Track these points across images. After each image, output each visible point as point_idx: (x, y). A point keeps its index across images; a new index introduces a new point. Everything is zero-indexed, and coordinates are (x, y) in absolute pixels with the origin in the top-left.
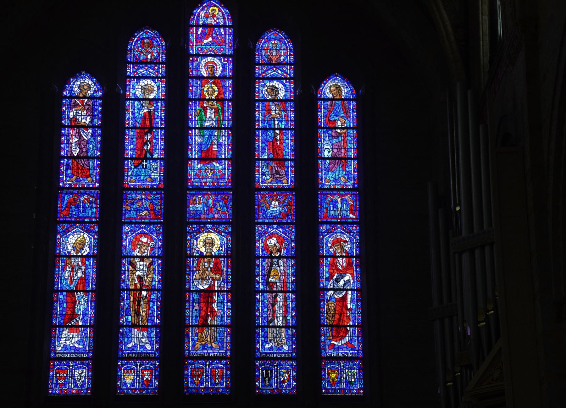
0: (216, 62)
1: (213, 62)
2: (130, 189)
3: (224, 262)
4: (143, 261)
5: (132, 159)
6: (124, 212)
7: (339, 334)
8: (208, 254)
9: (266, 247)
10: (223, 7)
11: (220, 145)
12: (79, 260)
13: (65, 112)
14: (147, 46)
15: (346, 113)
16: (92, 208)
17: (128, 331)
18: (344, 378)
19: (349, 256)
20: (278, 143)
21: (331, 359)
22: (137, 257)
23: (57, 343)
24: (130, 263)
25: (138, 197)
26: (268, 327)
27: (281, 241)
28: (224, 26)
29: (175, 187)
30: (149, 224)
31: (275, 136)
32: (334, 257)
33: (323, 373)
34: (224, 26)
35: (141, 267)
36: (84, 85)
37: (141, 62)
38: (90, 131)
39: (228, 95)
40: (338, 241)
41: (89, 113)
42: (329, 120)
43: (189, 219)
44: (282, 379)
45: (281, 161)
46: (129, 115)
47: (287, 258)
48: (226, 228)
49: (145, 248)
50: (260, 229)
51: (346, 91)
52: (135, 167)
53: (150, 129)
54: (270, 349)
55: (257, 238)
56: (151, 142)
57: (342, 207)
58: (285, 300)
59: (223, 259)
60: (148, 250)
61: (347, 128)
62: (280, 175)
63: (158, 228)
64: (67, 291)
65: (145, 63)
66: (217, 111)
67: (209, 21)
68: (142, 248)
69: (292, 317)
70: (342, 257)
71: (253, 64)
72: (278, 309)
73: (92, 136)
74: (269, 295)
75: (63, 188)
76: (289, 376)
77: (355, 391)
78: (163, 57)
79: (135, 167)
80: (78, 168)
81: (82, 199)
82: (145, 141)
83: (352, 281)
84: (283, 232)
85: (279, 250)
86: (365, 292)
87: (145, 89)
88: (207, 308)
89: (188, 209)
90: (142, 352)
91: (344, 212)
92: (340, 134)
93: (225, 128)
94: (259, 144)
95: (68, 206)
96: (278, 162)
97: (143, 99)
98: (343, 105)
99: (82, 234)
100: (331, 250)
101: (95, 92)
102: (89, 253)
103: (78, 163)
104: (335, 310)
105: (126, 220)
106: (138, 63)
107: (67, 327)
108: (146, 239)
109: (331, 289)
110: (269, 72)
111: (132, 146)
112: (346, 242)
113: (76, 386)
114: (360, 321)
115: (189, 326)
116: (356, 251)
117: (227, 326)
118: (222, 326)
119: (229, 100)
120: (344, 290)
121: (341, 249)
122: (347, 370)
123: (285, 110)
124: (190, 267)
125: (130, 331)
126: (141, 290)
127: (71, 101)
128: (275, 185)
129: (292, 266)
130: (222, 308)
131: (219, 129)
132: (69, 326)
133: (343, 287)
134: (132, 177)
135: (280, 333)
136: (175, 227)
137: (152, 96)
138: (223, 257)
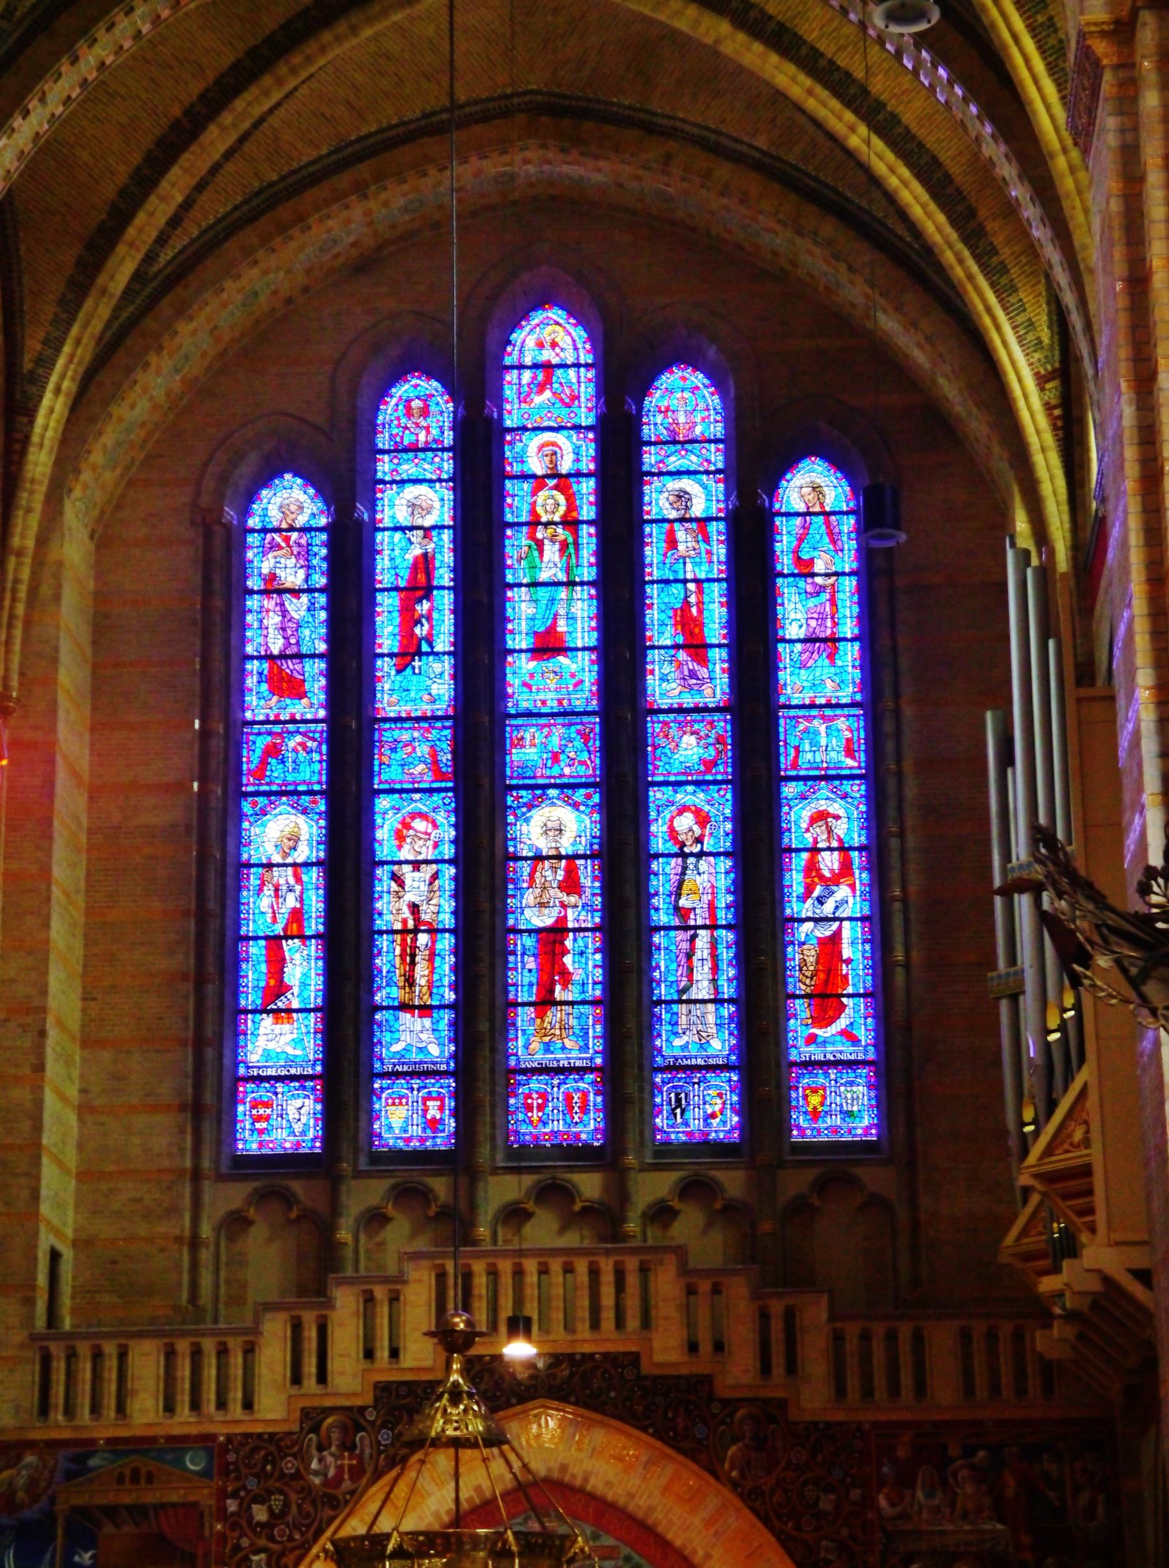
1: (554, 444)
5: (391, 655)
6: (376, 768)
7: (826, 1011)
8: (553, 852)
9: (673, 834)
11: (571, 618)
14: (417, 411)
15: (833, 542)
16: (311, 761)
17: (391, 1018)
19: (843, 849)
20: (694, 610)
21: (810, 1065)
22: (407, 862)
23: (250, 1047)
24: (395, 877)
26: (680, 1001)
27: (703, 820)
28: (577, 365)
30: (430, 791)
31: (686, 597)
32: (814, 850)
33: (794, 1095)
34: (577, 365)
35: (415, 882)
37: (406, 450)
38: (304, 598)
39: (587, 512)
40: (821, 816)
41: (302, 562)
42: (799, 558)
43: (512, 778)
45: (697, 647)
46: (382, 562)
47: (716, 855)
48: (588, 796)
49: (421, 842)
50: (659, 795)
51: (833, 494)
52: (399, 672)
54: (685, 1047)
55: (653, 815)
56: (429, 618)
59: (582, 862)
61: (837, 574)
63: (447, 801)
64: (266, 938)
65: (414, 448)
66: (564, 546)
67: (547, 355)
68: (415, 841)
69: (730, 980)
74: (681, 935)
75: (254, 723)
76: (724, 1103)
77: (860, 1131)
78: (448, 438)
79: (399, 672)
80: (281, 679)
81: (292, 744)
83: (851, 900)
84: (708, 802)
85: (699, 840)
86: (879, 926)
87: (415, 507)
88: (553, 965)
89: (508, 758)
90: (421, 1062)
91: (833, 754)
92: (822, 588)
93: (582, 584)
94: (653, 616)
95: (264, 762)
98: (827, 524)
99: (293, 818)
100: (808, 835)
101: (314, 515)
103: (280, 669)
104: (817, 963)
105: (382, 786)
106: (398, 449)
107: (268, 1012)
109: (808, 919)
110: (672, 459)
111: (390, 629)
113: (293, 1133)
114: (869, 985)
115: (516, 1004)
117: (594, 1003)
118: (583, 1002)
120: (835, 919)
123: (707, 540)
125: (397, 1019)
126: (416, 931)
128: (688, 701)
129: (727, 873)
130: (584, 964)
131: (570, 584)
137: (428, 522)
138: (584, 857)
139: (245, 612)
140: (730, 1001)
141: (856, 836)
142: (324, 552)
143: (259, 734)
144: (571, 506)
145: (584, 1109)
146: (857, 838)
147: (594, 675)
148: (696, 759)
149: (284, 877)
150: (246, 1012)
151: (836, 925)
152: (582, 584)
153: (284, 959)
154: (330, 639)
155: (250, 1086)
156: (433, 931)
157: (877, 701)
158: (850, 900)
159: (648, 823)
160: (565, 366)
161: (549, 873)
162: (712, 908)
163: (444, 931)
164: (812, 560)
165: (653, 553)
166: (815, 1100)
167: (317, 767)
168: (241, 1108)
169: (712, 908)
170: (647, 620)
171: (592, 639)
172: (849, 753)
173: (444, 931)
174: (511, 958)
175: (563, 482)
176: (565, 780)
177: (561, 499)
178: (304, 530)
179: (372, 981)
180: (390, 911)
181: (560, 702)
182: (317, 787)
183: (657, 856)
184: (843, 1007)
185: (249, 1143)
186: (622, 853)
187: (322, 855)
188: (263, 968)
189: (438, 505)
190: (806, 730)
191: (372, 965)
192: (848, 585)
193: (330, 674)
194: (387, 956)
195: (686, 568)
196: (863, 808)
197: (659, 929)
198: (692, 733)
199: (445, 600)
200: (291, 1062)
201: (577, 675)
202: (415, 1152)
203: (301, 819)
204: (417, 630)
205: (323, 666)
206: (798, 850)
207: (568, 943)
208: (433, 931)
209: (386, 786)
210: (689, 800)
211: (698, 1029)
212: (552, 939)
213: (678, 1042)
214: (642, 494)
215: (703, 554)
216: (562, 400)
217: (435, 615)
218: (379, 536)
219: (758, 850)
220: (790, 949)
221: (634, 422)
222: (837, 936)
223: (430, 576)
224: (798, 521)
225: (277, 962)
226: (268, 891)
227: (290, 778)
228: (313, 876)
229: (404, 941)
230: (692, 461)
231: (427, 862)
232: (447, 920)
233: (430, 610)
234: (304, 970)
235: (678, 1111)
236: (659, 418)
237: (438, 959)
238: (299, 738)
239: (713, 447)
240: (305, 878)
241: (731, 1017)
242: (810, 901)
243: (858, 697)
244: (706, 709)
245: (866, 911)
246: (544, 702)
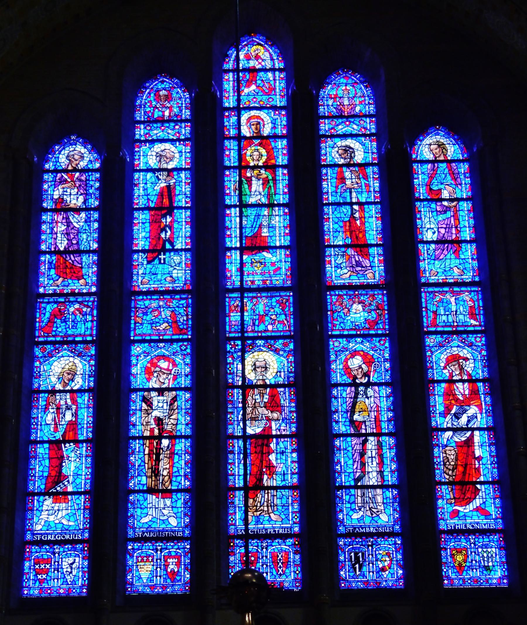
0: (262, 117)
1: (258, 117)
2: (141, 293)
3: (285, 393)
4: (163, 395)
6: (132, 326)
7: (464, 494)
8: (260, 383)
9: (347, 370)
10: (271, 46)
13: (47, 191)
15: (455, 179)
16: (86, 321)
17: (141, 498)
20: (358, 222)
21: (455, 532)
22: (154, 389)
23: (36, 519)
24: (145, 400)
25: (154, 304)
26: (356, 487)
27: (368, 360)
28: (273, 70)
29: (208, 289)
30: (171, 341)
31: (352, 214)
34: (273, 70)
36: (76, 154)
37: (156, 121)
38: (83, 215)
39: (282, 160)
41: (82, 191)
42: (431, 189)
43: (230, 332)
44: (381, 566)
45: (362, 247)
46: (138, 191)
47: (379, 384)
48: (285, 345)
49: (165, 376)
50: (336, 344)
51: (453, 149)
52: (149, 262)
53: (170, 210)
55: (333, 357)
56: (171, 227)
57: (457, 309)
58: (380, 446)
59: (282, 389)
60: (169, 380)
62: (362, 267)
63: (183, 348)
64: (49, 442)
65: (161, 121)
66: (266, 181)
67: (252, 63)
68: (160, 376)
69: (392, 472)
70: (463, 381)
72: (370, 460)
73: (86, 221)
74: (355, 441)
75: (44, 295)
76: (391, 560)
77: (495, 581)
78: (186, 114)
79: (149, 262)
81: (72, 310)
82: (162, 225)
84: (372, 349)
85: (367, 375)
86: (501, 433)
87: (162, 157)
88: (262, 462)
89: (227, 319)
90: (163, 530)
91: (461, 317)
92: (448, 209)
93: (279, 205)
94: (330, 226)
95: (51, 321)
96: (358, 249)
97: (160, 170)
98: (450, 169)
99: (71, 359)
100: (445, 371)
101: (91, 161)
102: (82, 386)
103: (65, 261)
104: (457, 459)
105: (136, 338)
106: (150, 121)
108: (167, 363)
109: (448, 429)
110: (340, 127)
111: (143, 234)
112: (466, 359)
114: (496, 475)
116: (483, 372)
118: (284, 487)
119: (283, 167)
120: (468, 429)
121: (461, 370)
122: (480, 550)
123: (366, 177)
124: (232, 402)
125: (146, 499)
126: (160, 437)
127: (56, 177)
128: (355, 280)
129: (388, 397)
130: (284, 461)
131: (270, 205)
132: (53, 494)
133: (467, 425)
135: (374, 497)
136: (209, 344)
137: (171, 166)
139: (41, 222)
140: (393, 486)
142: (97, 185)
143: (48, 303)
144: (270, 156)
145: (286, 564)
146: (480, 374)
147: (288, 265)
148: (362, 320)
149: (65, 400)
150: (33, 494)
151: (469, 434)
152: (279, 205)
153: (63, 457)
154: (99, 241)
155: (34, 549)
156: (173, 437)
157: (492, 282)
158: (477, 415)
159: (330, 363)
160: (265, 70)
161: (258, 397)
162: (378, 421)
163: (181, 437)
164: (440, 190)
165: (328, 186)
166: (460, 558)
167: (89, 325)
168: (27, 564)
169: (378, 421)
170: (325, 228)
171: (286, 241)
172: (472, 315)
173: (181, 437)
174: (231, 456)
175: (265, 141)
176: (269, 334)
177: (263, 152)
178: (83, 171)
179: (127, 471)
180: (141, 423)
181: (264, 282)
182: (89, 338)
183: (337, 385)
185: (32, 589)
186: (311, 383)
187: (92, 384)
188: (47, 463)
189: (179, 156)
190: (441, 301)
191: (127, 461)
192: (465, 206)
193: (99, 264)
194: (139, 455)
195: (352, 194)
196: (484, 353)
197: (339, 436)
198: (359, 303)
199: (183, 216)
200: (65, 530)
201: (275, 265)
202: (158, 595)
203: (77, 360)
204: (163, 235)
205: (95, 258)
206: (439, 382)
207: (273, 446)
208: (173, 437)
209: (140, 338)
210: (359, 347)
211: (370, 506)
213: (355, 516)
214: (320, 148)
215: (364, 187)
216: (263, 91)
217: (176, 225)
218: (136, 175)
219: (410, 383)
220: (436, 450)
221: (314, 102)
222: (470, 441)
223: (171, 199)
224: (430, 166)
225: (57, 459)
227: (70, 332)
228: (84, 399)
229: (151, 444)
230: (354, 128)
231: (169, 389)
232: (183, 429)
233: (172, 222)
234: (77, 466)
235: (357, 566)
236: (330, 102)
237: (176, 457)
238: (77, 306)
239: (368, 120)
240: (79, 400)
241: (394, 498)
242: (449, 417)
243: (477, 279)
244: (368, 287)
245: (491, 424)
246: (253, 282)
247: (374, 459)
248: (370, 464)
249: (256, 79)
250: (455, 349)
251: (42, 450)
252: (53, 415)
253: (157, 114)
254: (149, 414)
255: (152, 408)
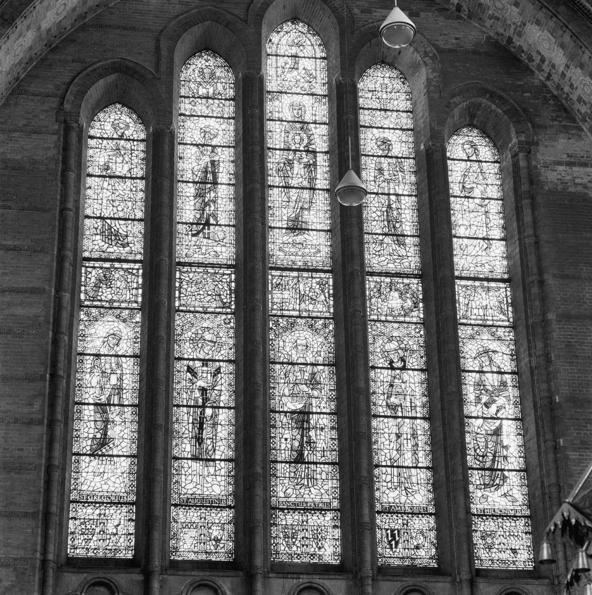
4: (207, 366)
7: (494, 480)
12: (113, 361)
18: (506, 545)
24: (190, 370)
42: (464, 187)
45: (399, 237)
48: (325, 326)
56: (214, 202)
66: (307, 166)
71: (355, 109)
82: (206, 200)
95: (97, 287)
96: (395, 238)
103: (110, 228)
120: (498, 419)
126: (204, 406)
133: (496, 414)
134: (187, 247)
141: (508, 364)
143: (94, 268)
151: (498, 422)
161: (299, 374)
164: (472, 188)
184: (504, 478)
189: (224, 132)
198: (396, 290)
203: (122, 326)
212: (302, 418)
221: (354, 92)
222: (497, 432)
226: (97, 372)
235: (393, 542)
247: (409, 441)
248: (405, 445)
249: (295, 62)
250: (485, 341)
251: (88, 412)
252: (99, 378)
253: (202, 91)
254: (193, 384)
255: (196, 378)
